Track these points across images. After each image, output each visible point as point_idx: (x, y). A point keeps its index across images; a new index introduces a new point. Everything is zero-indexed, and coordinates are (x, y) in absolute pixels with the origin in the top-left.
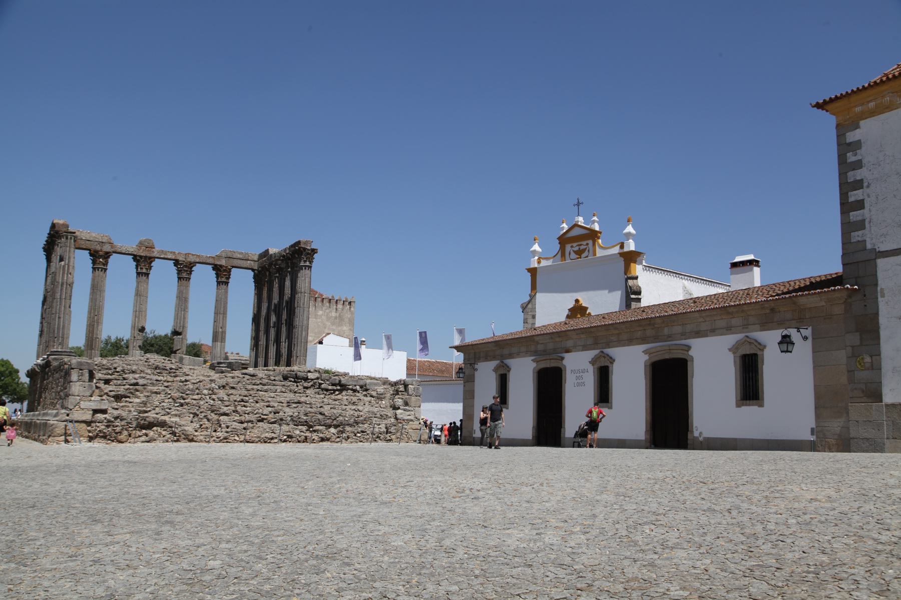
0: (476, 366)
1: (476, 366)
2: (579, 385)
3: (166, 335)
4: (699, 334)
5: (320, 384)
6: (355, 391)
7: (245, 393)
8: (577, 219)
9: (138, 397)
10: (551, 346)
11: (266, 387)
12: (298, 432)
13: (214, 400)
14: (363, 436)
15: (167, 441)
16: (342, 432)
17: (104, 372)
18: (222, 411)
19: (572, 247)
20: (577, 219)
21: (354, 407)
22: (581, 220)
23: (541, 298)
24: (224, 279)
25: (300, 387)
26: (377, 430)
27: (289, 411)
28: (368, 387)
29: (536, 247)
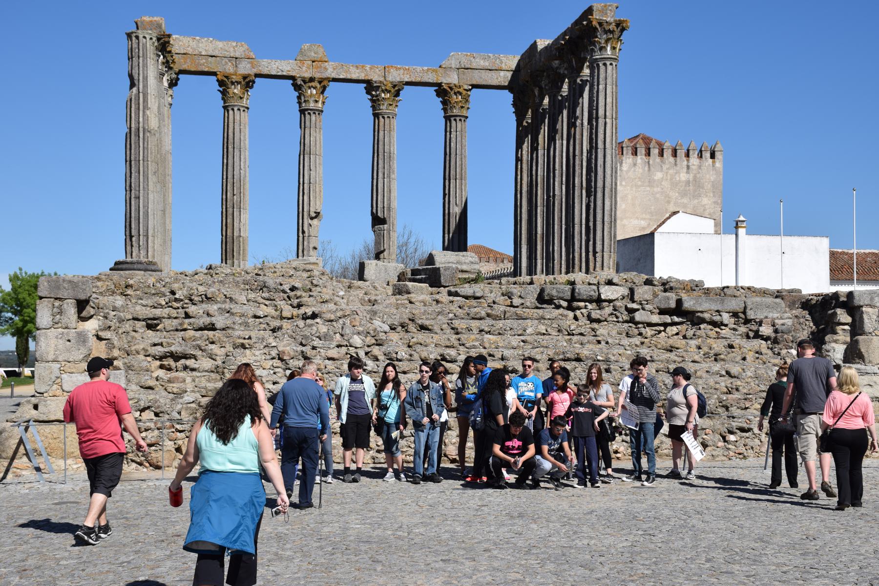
11: (500, 324)
17: (150, 302)
21: (717, 367)
25: (583, 321)
28: (751, 315)
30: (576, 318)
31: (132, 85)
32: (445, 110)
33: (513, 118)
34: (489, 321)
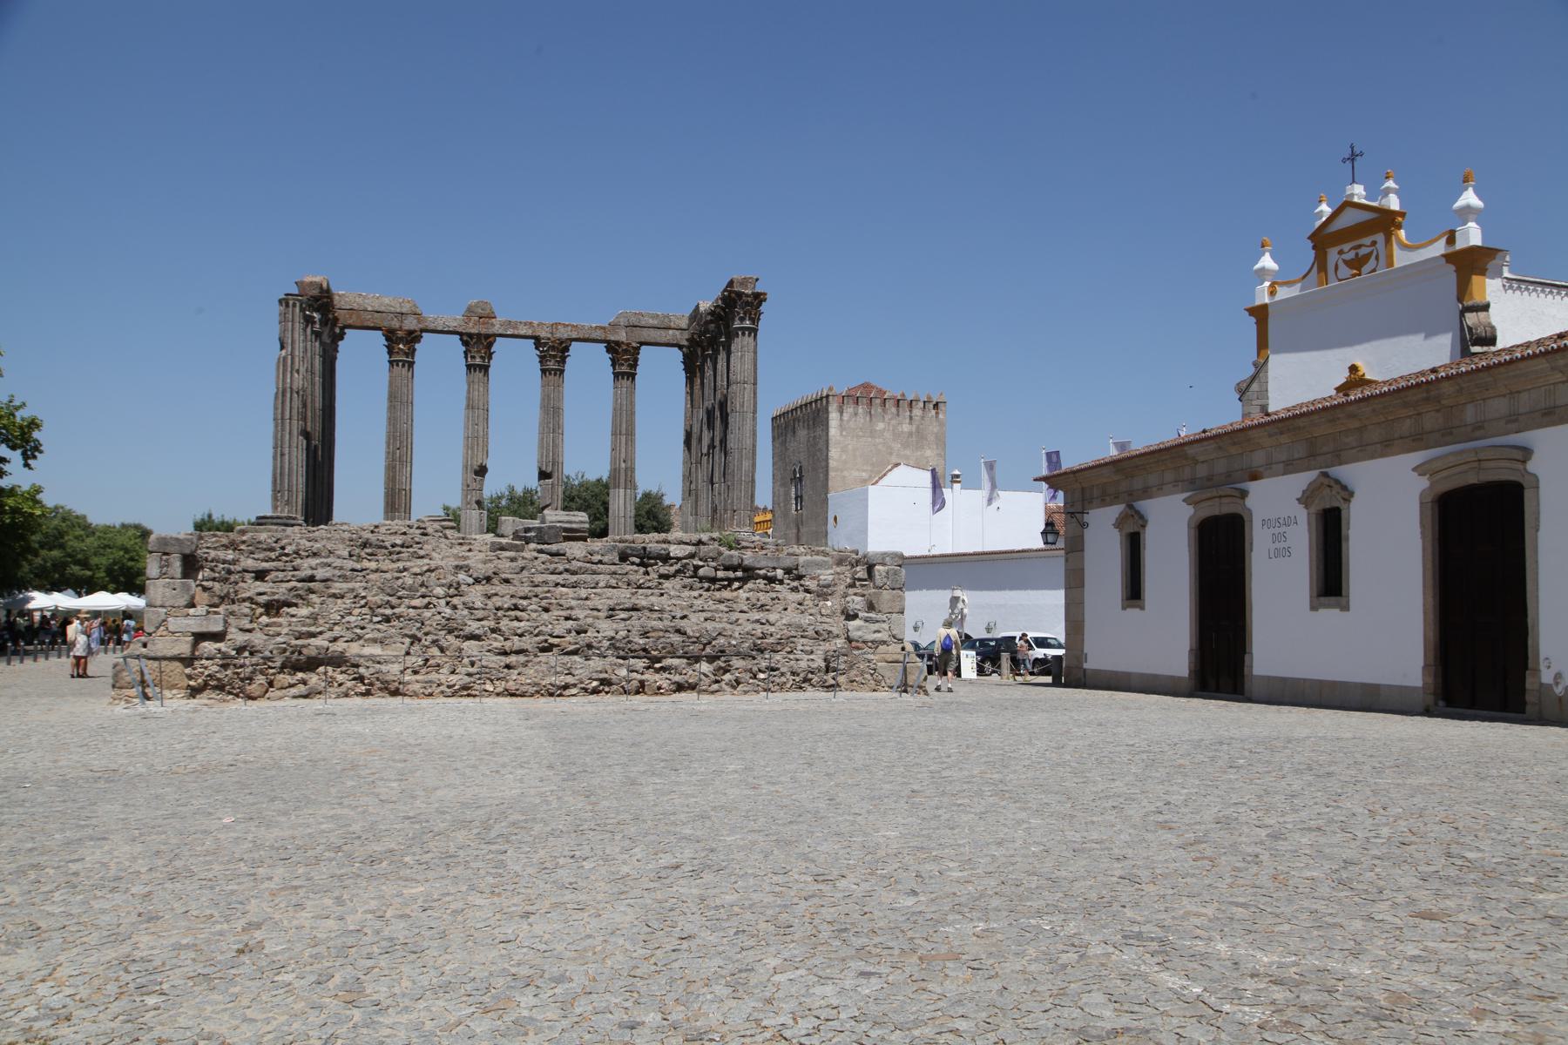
2: (1278, 553)
3: (599, 481)
4: (1551, 415)
5: (697, 568)
6: (771, 580)
7: (526, 590)
8: (1349, 190)
9: (309, 604)
10: (1221, 467)
11: (574, 578)
12: (623, 672)
13: (455, 608)
15: (347, 695)
16: (726, 671)
17: (261, 556)
18: (467, 630)
19: (1341, 252)
20: (1349, 190)
21: (756, 615)
22: (1358, 192)
24: (624, 369)
25: (654, 575)
26: (803, 664)
27: (607, 628)
28: (802, 571)
29: (1267, 262)
30: (647, 573)
31: (282, 347)
32: (613, 365)
34: (566, 576)
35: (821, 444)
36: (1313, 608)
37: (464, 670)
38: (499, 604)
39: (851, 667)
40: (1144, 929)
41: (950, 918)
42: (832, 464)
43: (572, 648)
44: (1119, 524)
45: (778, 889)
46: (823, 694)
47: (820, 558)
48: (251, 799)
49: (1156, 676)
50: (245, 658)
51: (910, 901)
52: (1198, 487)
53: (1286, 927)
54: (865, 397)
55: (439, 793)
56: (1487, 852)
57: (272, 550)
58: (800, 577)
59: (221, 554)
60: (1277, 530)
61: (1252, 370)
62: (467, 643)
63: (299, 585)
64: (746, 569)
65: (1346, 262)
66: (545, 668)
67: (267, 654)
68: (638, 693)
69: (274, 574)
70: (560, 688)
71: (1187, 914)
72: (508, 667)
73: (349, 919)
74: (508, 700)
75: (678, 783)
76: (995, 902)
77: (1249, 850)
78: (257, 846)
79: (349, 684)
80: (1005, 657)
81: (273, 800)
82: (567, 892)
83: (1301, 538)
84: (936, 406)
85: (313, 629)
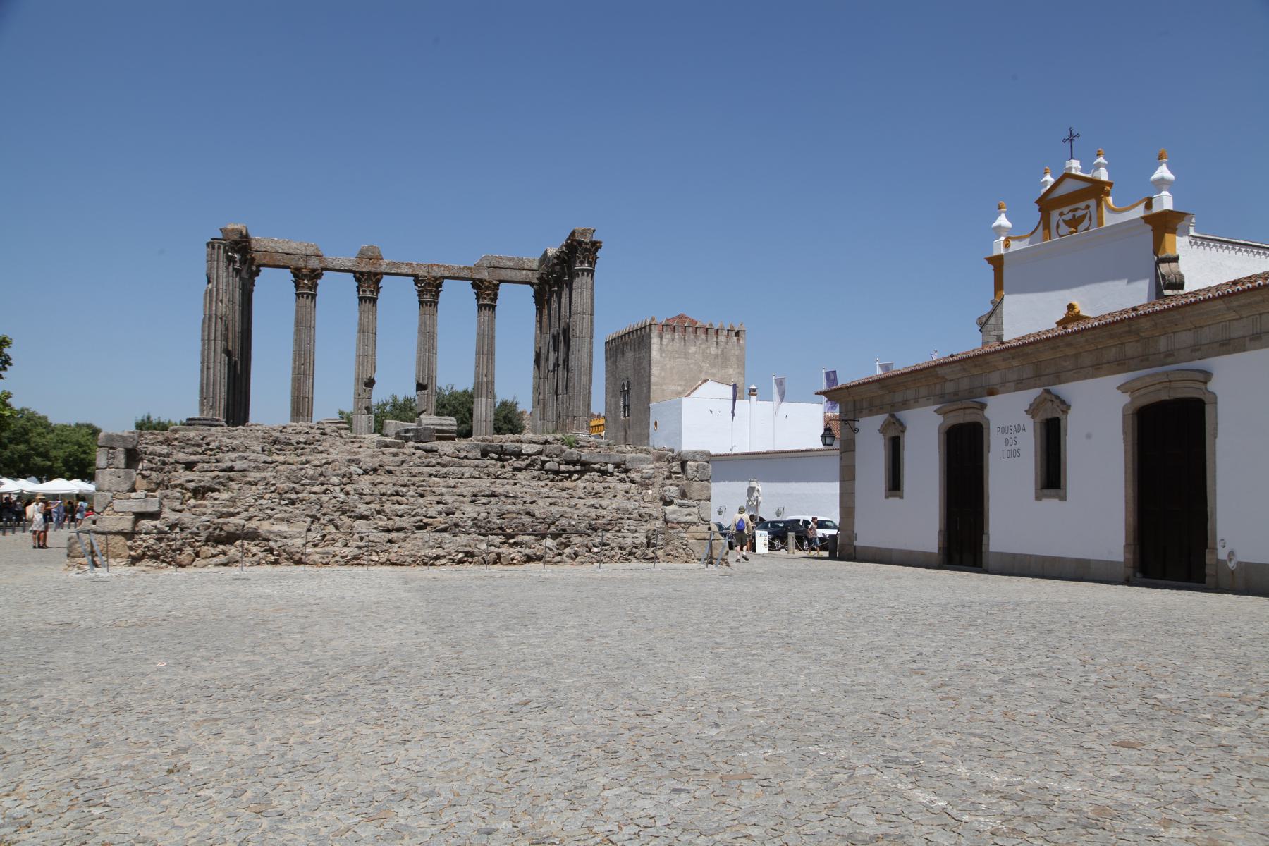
0: (857, 425)
1: (857, 425)
2: (1010, 454)
4: (1228, 346)
5: (544, 462)
6: (604, 473)
7: (405, 479)
9: (229, 490)
10: (965, 384)
11: (445, 470)
12: (484, 546)
13: (348, 493)
14: (603, 553)
15: (259, 564)
16: (567, 546)
17: (190, 450)
18: (358, 512)
19: (1061, 214)
21: (591, 501)
22: (1075, 166)
23: (1011, 303)
24: (487, 301)
25: (509, 468)
26: (629, 541)
27: (471, 510)
28: (629, 466)
29: (1003, 221)
30: (503, 466)
31: (209, 282)
32: (478, 299)
33: (532, 308)
34: (438, 468)
35: (645, 364)
36: (1038, 498)
37: (354, 544)
38: (383, 491)
39: (667, 544)
40: (900, 754)
41: (746, 745)
42: (653, 379)
43: (442, 526)
44: (883, 430)
45: (607, 722)
46: (645, 565)
47: (643, 455)
48: (179, 648)
49: (911, 552)
50: (177, 534)
51: (713, 732)
52: (946, 400)
53: (1014, 754)
54: (681, 326)
55: (333, 643)
56: (1174, 694)
57: (199, 445)
58: (627, 471)
59: (158, 449)
60: (1009, 436)
61: (990, 307)
62: (357, 522)
63: (221, 474)
64: (584, 464)
65: (1065, 222)
66: (420, 543)
67: (194, 530)
68: (495, 563)
69: (200, 465)
70: (432, 558)
71: (935, 742)
72: (390, 541)
73: (259, 745)
74: (390, 568)
75: (527, 636)
76: (782, 733)
77: (985, 692)
78: (184, 685)
79: (261, 555)
80: (791, 537)
81: (198, 648)
82: (436, 724)
83: (1029, 442)
84: (737, 334)
85: (232, 510)
